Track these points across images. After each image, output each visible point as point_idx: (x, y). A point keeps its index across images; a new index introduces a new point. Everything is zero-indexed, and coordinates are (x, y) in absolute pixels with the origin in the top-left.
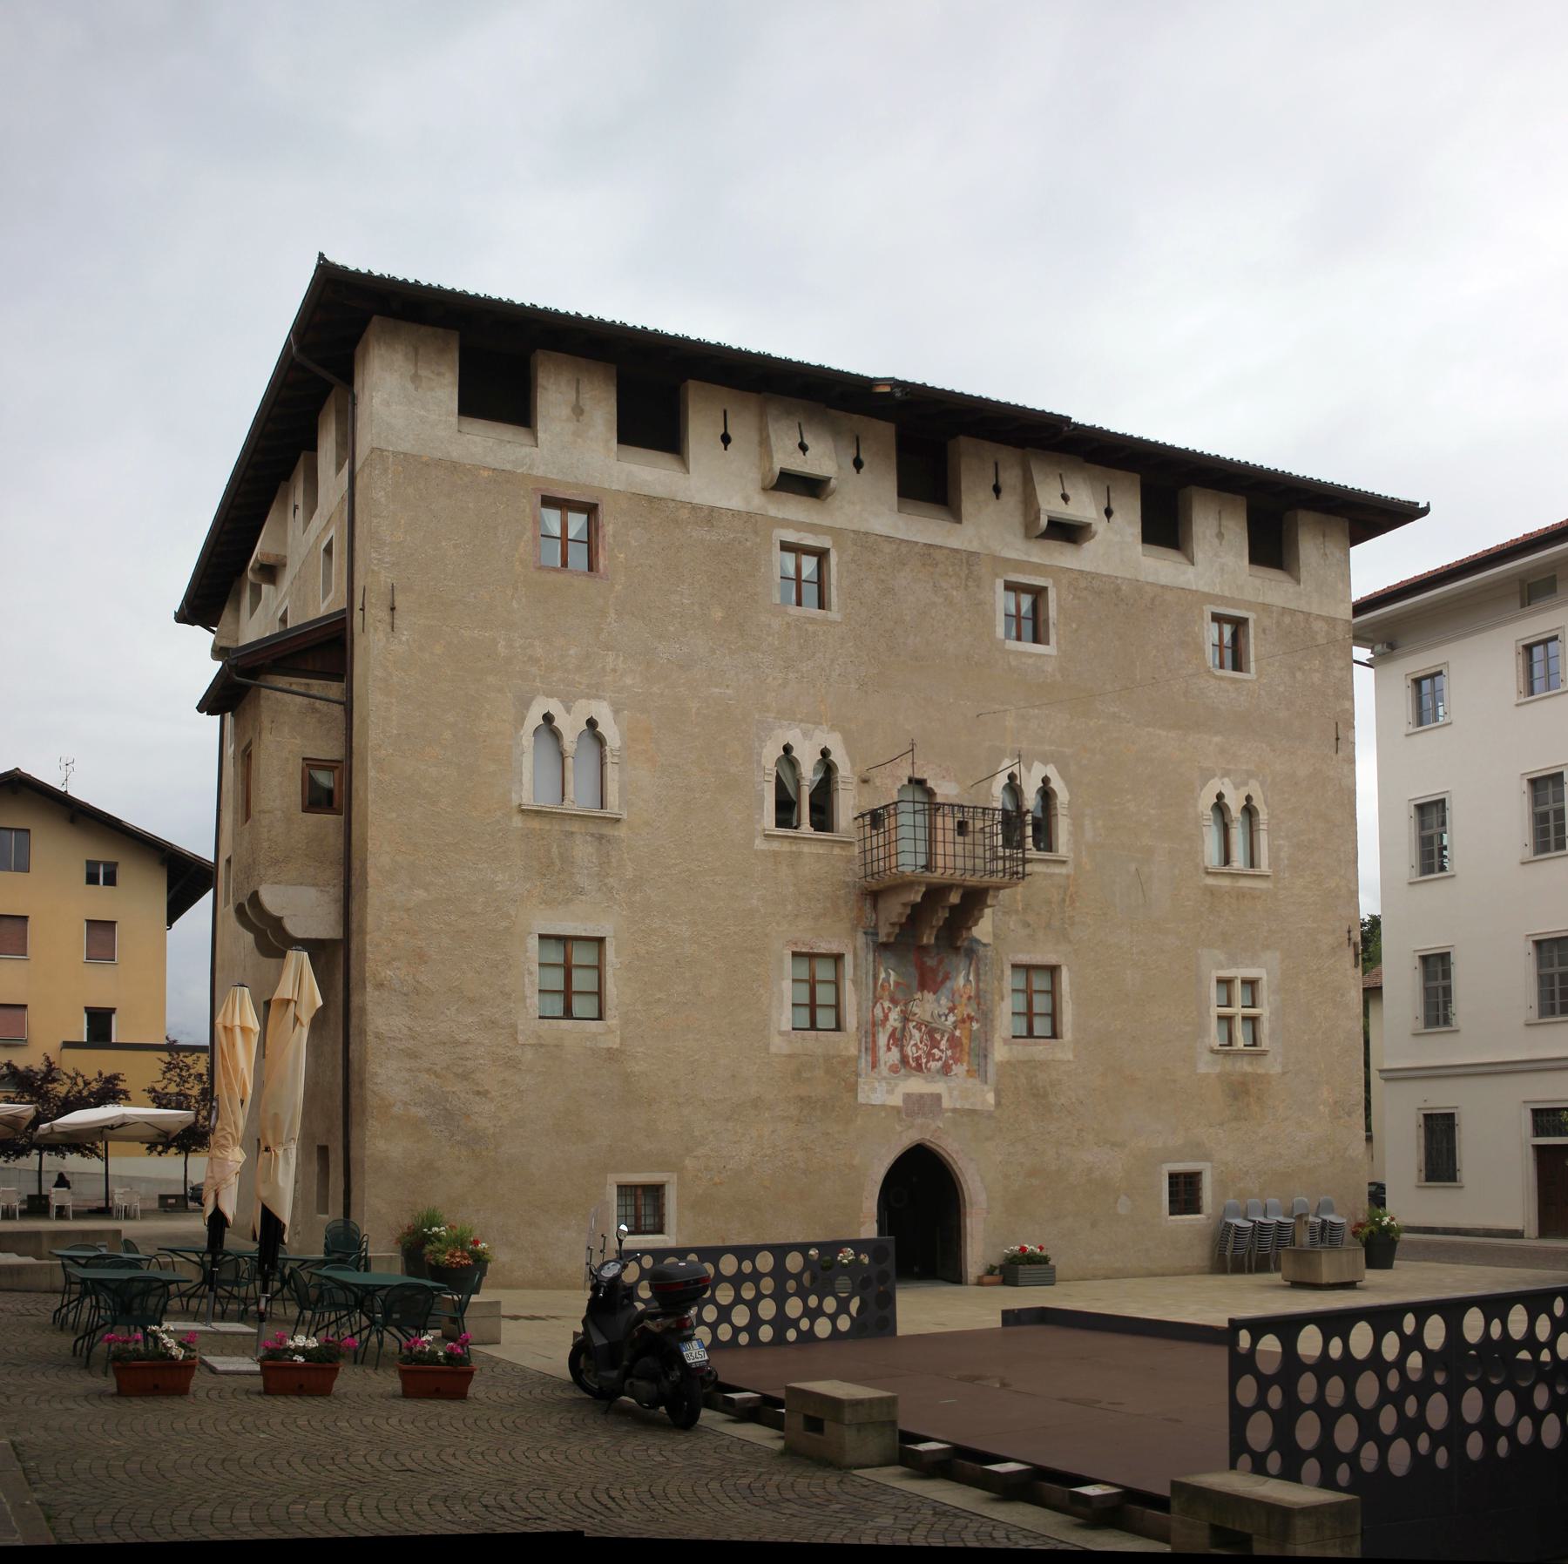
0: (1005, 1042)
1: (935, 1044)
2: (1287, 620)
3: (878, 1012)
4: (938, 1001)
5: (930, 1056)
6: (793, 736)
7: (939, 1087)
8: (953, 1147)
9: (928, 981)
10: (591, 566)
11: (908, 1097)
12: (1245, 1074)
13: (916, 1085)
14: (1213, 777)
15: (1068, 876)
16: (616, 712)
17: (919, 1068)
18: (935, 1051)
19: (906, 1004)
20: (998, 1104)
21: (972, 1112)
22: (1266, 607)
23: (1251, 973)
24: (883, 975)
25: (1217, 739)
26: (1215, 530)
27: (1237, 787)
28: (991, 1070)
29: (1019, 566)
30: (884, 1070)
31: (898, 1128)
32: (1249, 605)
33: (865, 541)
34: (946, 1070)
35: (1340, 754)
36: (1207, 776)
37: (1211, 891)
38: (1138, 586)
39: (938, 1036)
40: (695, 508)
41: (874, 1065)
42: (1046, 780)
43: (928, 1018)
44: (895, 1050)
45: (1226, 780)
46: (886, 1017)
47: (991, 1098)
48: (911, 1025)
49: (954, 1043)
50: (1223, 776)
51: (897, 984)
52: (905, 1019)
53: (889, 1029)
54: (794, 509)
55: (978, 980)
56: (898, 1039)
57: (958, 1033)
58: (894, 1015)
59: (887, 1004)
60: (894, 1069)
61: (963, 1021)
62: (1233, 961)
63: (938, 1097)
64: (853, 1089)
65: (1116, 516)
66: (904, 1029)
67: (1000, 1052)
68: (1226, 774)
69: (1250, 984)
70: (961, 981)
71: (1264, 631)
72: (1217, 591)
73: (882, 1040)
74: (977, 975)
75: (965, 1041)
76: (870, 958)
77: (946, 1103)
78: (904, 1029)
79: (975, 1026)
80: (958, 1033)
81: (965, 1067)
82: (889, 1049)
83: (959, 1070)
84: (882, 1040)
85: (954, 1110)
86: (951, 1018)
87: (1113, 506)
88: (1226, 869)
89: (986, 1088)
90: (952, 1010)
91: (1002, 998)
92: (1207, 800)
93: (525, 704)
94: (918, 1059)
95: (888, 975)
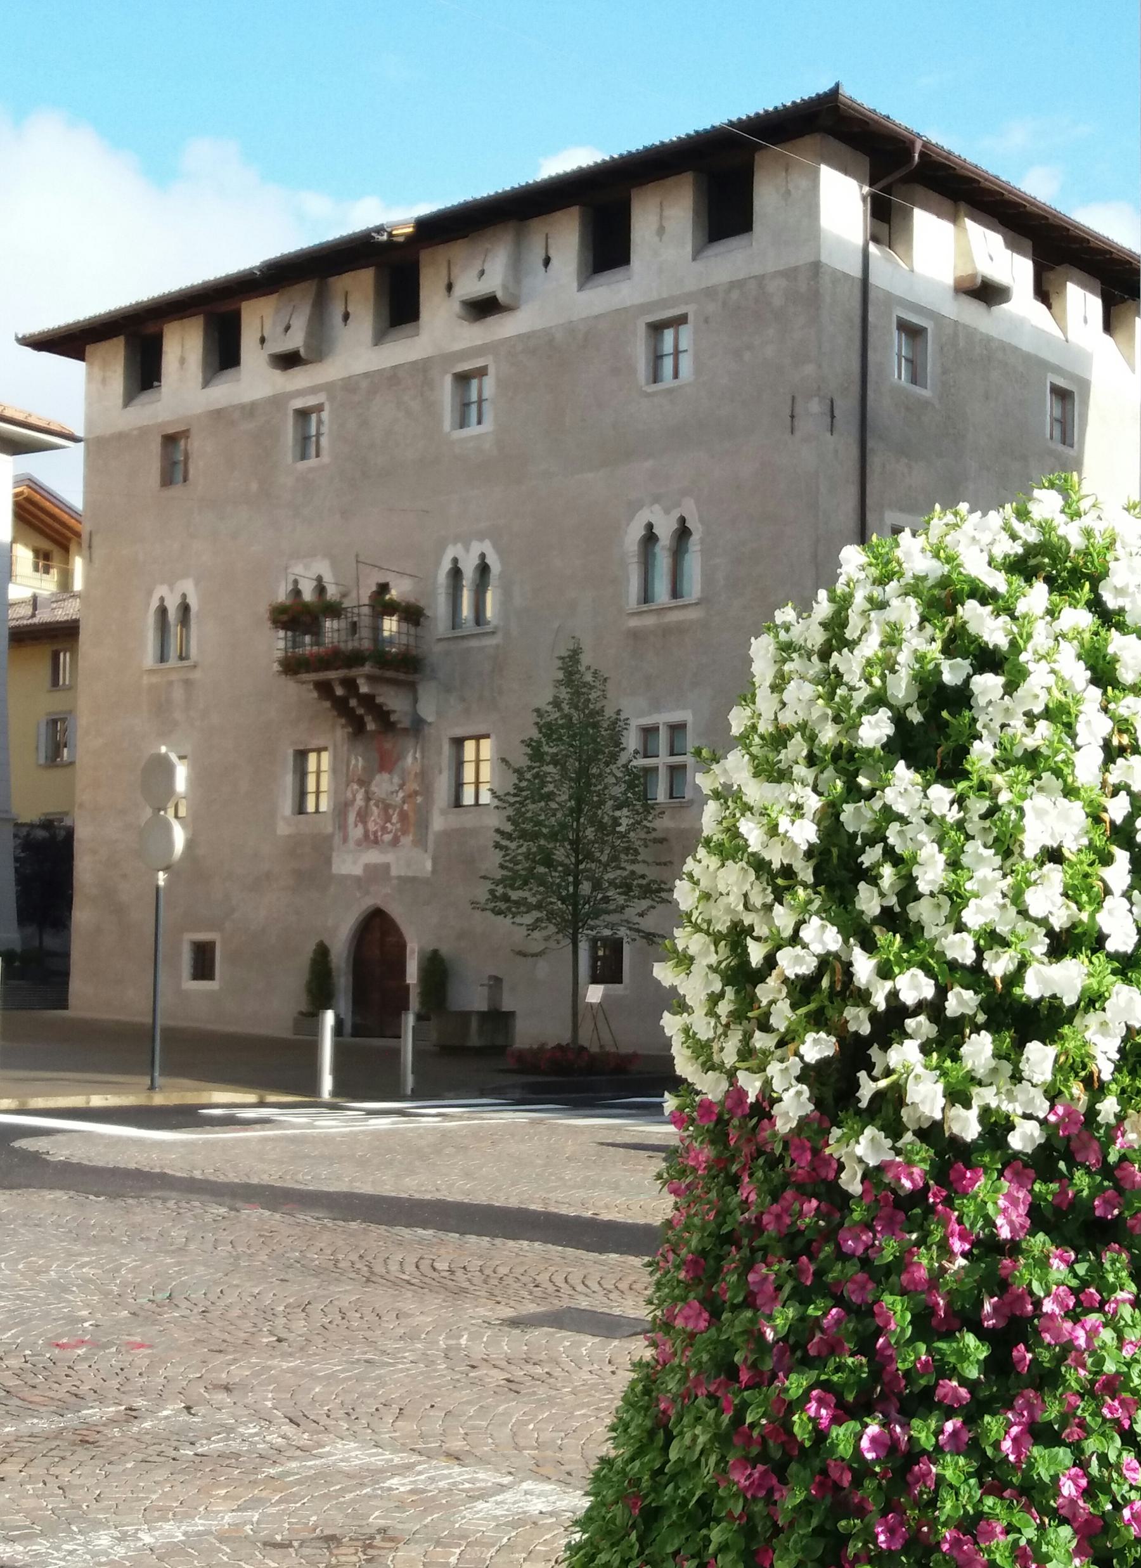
0: (443, 812)
1: (388, 819)
2: (735, 295)
3: (349, 795)
4: (391, 779)
5: (384, 829)
6: (298, 569)
7: (388, 857)
8: (396, 911)
9: (386, 763)
10: (185, 480)
11: (367, 867)
12: (668, 830)
13: (373, 857)
14: (641, 507)
15: (497, 646)
16: (197, 584)
17: (376, 842)
18: (388, 825)
19: (369, 783)
20: (434, 871)
21: (413, 879)
22: (710, 292)
23: (676, 717)
24: (353, 762)
25: (649, 464)
26: (654, 227)
27: (667, 511)
28: (431, 838)
29: (464, 355)
30: (351, 844)
31: (358, 895)
32: (688, 298)
33: (349, 385)
34: (395, 842)
35: (798, 434)
36: (634, 507)
37: (636, 635)
38: (570, 329)
39: (391, 811)
40: (242, 407)
41: (345, 839)
42: (483, 556)
43: (383, 796)
44: (360, 827)
45: (657, 507)
46: (354, 796)
47: (429, 865)
48: (372, 802)
49: (403, 817)
50: (652, 504)
51: (364, 768)
52: (368, 799)
53: (356, 807)
54: (299, 379)
55: (423, 757)
56: (363, 816)
57: (406, 807)
58: (360, 796)
59: (355, 787)
60: (359, 843)
61: (410, 796)
62: (656, 706)
63: (387, 867)
64: (328, 862)
65: (554, 262)
66: (367, 806)
67: (438, 823)
68: (656, 499)
69: (677, 729)
70: (409, 760)
71: (706, 321)
72: (654, 296)
73: (352, 817)
74: (423, 752)
75: (411, 814)
76: (345, 748)
77: (394, 872)
78: (367, 806)
79: (419, 799)
80: (406, 807)
81: (411, 838)
82: (356, 826)
83: (406, 840)
84: (352, 817)
85: (399, 878)
86: (401, 794)
87: (552, 253)
88: (680, 602)
89: (426, 856)
90: (401, 786)
91: (440, 772)
92: (635, 533)
93: (150, 593)
94: (375, 833)
95: (357, 760)
